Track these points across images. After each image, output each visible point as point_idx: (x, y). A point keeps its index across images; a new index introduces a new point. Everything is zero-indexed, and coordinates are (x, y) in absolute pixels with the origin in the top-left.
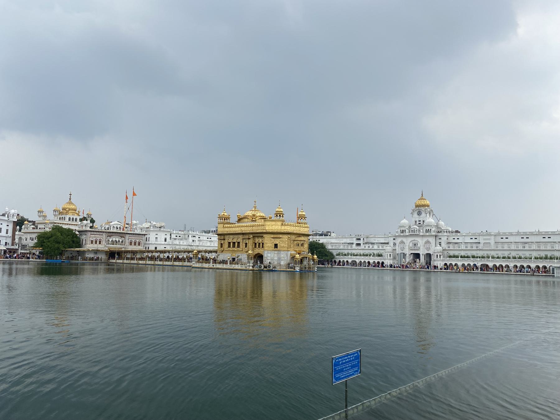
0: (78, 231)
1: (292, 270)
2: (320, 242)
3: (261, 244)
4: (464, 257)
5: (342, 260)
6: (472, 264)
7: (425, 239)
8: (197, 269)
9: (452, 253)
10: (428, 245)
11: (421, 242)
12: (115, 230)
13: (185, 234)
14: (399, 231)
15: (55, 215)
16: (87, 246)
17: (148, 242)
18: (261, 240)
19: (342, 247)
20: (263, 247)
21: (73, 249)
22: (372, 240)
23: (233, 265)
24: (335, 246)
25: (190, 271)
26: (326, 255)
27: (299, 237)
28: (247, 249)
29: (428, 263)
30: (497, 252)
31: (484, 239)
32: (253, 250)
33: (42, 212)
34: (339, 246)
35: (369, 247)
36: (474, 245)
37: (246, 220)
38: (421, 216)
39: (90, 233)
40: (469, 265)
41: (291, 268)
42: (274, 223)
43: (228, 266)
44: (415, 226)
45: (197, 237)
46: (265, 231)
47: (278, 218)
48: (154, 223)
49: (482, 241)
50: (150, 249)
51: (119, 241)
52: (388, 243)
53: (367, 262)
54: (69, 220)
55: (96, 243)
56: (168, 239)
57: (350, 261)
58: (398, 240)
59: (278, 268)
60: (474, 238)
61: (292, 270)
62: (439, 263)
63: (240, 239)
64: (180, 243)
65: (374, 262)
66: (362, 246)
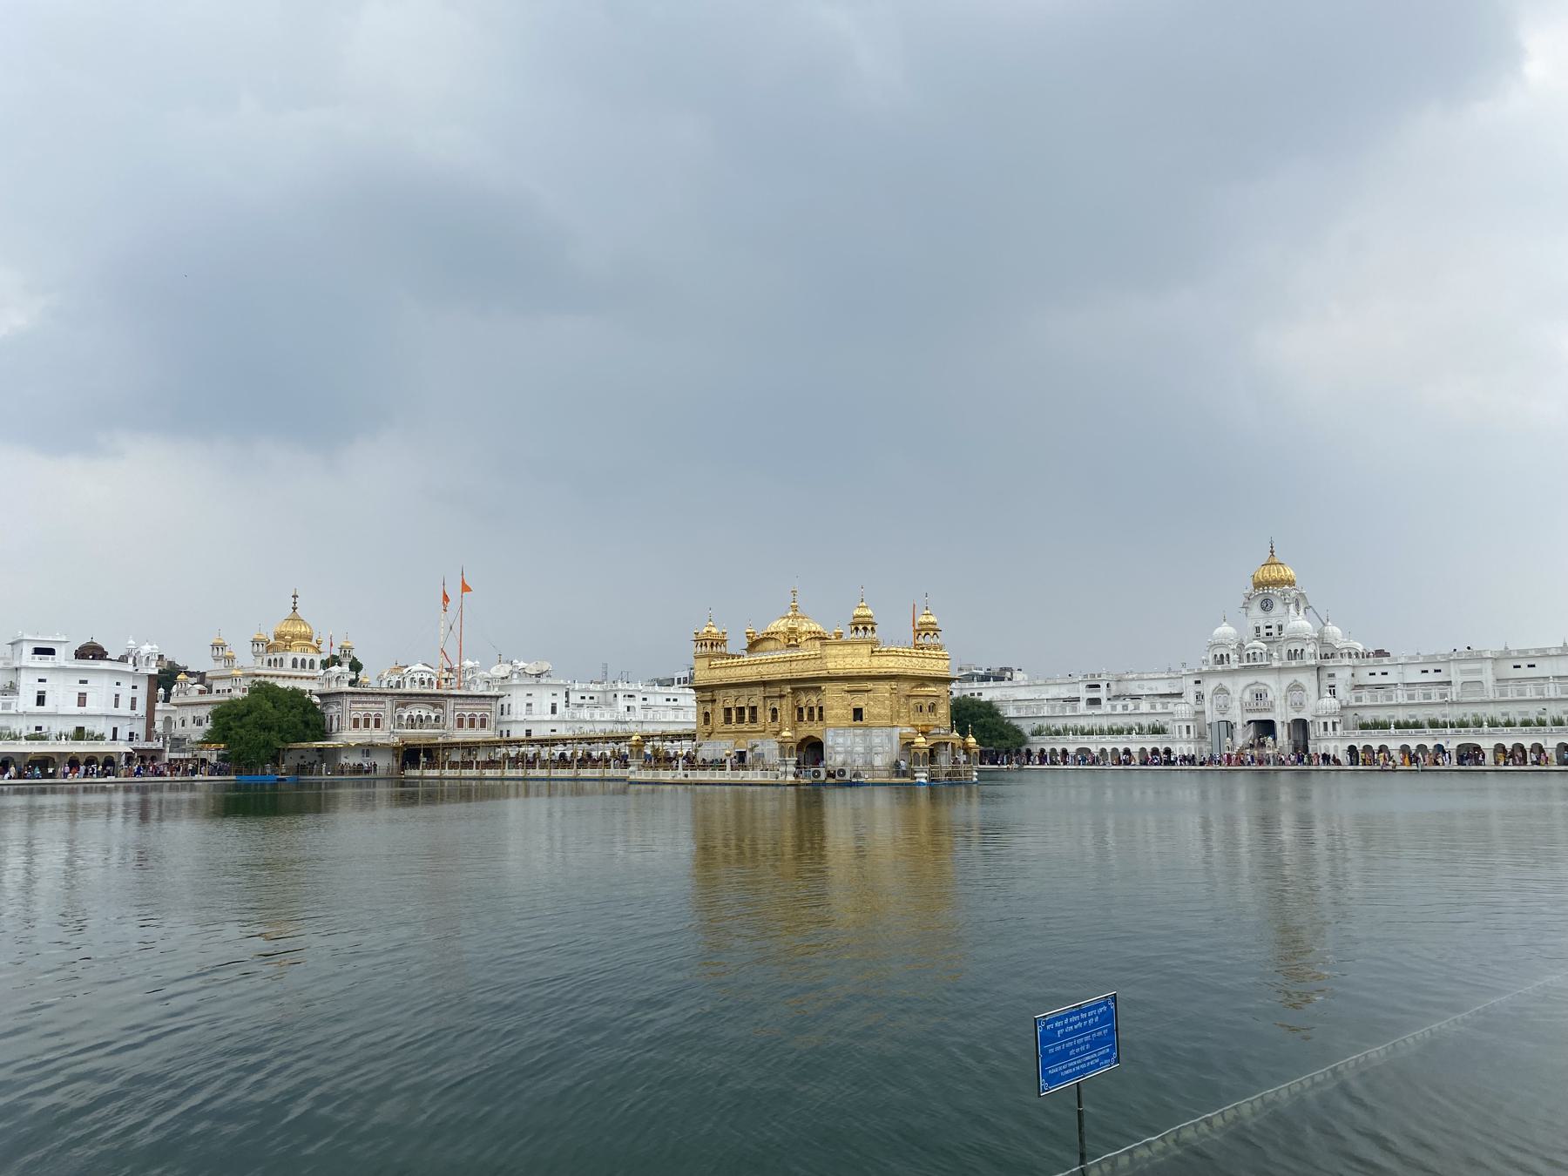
0: (320, 696)
1: (908, 780)
2: (984, 698)
3: (816, 711)
4: (1407, 726)
5: (1048, 749)
6: (1430, 745)
7: (1287, 679)
8: (643, 787)
9: (1368, 716)
10: (1296, 696)
11: (1275, 687)
12: (417, 689)
13: (605, 692)
14: (1211, 657)
15: (256, 655)
16: (345, 733)
17: (506, 718)
18: (814, 699)
19: (1046, 711)
20: (821, 718)
21: (304, 744)
22: (1134, 688)
23: (742, 773)
25: (625, 792)
26: (1002, 736)
27: (923, 685)
28: (776, 724)
29: (1301, 749)
30: (1503, 708)
31: (1463, 672)
32: (794, 729)
33: (223, 646)
34: (1039, 708)
35: (1125, 707)
36: (1435, 694)
37: (771, 644)
38: (1273, 613)
39: (349, 699)
40: (1422, 748)
41: (904, 774)
42: (848, 649)
43: (727, 775)
44: (1256, 643)
45: (639, 697)
46: (824, 673)
47: (861, 634)
48: (522, 665)
49: (1457, 678)
50: (513, 736)
51: (428, 717)
52: (1179, 695)
53: (1059, 750)
54: (294, 665)
55: (367, 725)
56: (561, 708)
57: (1072, 749)
58: (1209, 686)
59: (866, 777)
60: (1431, 668)
61: (908, 780)
63: (756, 698)
64: (592, 715)
65: (1143, 750)
66: (1106, 707)
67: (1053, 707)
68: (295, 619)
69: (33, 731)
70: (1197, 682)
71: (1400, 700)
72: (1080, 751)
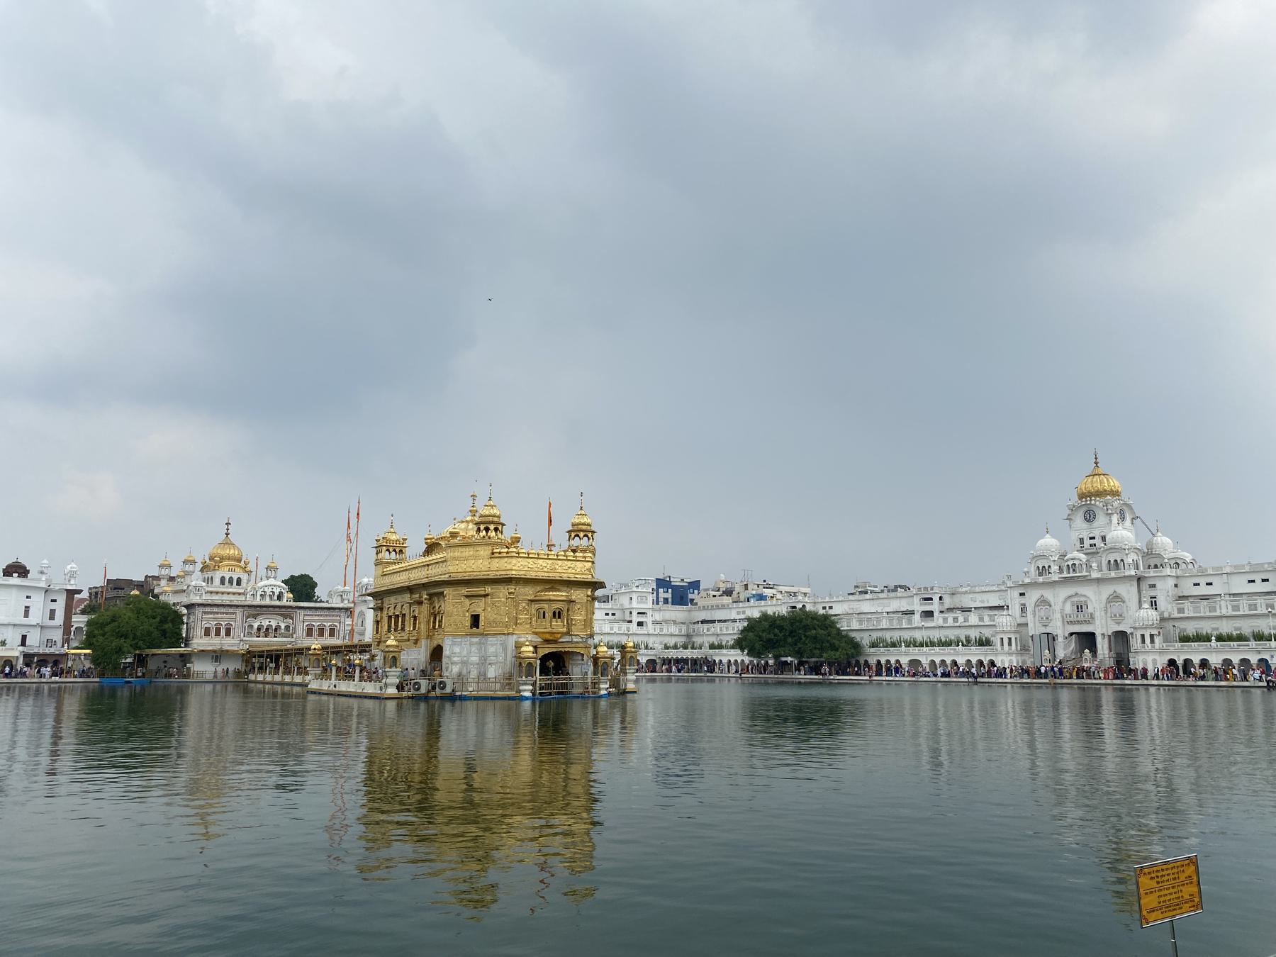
4: (1230, 638)
5: (883, 662)
7: (1107, 591)
9: (1191, 628)
10: (1116, 608)
11: (1095, 598)
12: (267, 602)
14: (1033, 569)
16: (195, 641)
19: (885, 624)
22: (967, 601)
24: (869, 620)
26: (834, 648)
32: (429, 637)
34: (879, 621)
35: (956, 620)
38: (1096, 524)
39: (201, 609)
40: (1245, 661)
42: (468, 552)
44: (1076, 554)
54: (222, 581)
55: (218, 632)
58: (1033, 596)
59: (471, 690)
62: (1150, 658)
66: (938, 620)
67: (891, 620)
68: (227, 543)
71: (1224, 612)
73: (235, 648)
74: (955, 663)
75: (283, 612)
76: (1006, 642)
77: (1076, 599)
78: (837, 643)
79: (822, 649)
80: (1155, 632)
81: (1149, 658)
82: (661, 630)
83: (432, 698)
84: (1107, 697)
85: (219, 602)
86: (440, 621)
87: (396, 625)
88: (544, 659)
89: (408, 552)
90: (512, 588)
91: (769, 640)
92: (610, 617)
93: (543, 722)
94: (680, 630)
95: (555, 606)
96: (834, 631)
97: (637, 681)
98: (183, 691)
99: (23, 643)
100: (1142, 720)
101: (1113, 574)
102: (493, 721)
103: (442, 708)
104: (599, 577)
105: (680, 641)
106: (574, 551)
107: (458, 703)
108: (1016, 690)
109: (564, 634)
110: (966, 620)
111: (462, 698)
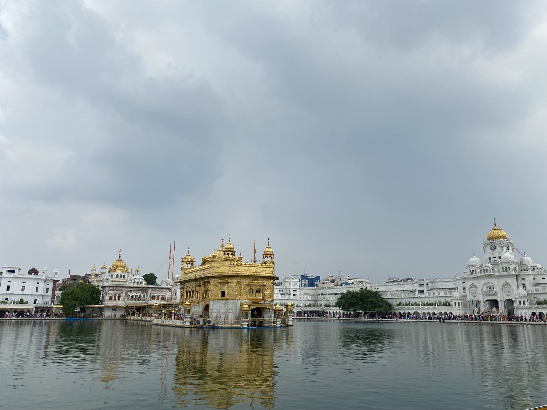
5: (402, 313)
7: (502, 281)
10: (507, 289)
11: (497, 284)
12: (136, 285)
19: (402, 296)
22: (439, 286)
24: (395, 294)
26: (380, 306)
32: (204, 301)
34: (400, 295)
35: (434, 294)
38: (496, 251)
42: (220, 264)
44: (487, 265)
54: (117, 276)
55: (115, 298)
57: (412, 312)
58: (468, 284)
59: (221, 324)
66: (426, 294)
67: (405, 294)
68: (120, 260)
69: (4, 300)
70: (464, 283)
72: (415, 312)
73: (122, 305)
74: (434, 313)
75: (142, 289)
76: (457, 304)
77: (488, 285)
78: (381, 304)
79: (375, 307)
80: (525, 300)
81: (523, 311)
82: (303, 298)
83: (205, 328)
84: (505, 330)
85: (116, 285)
86: (208, 294)
87: (190, 296)
88: (253, 311)
89: (195, 264)
90: (239, 280)
91: (351, 303)
92: (281, 292)
93: (252, 340)
94: (312, 298)
95: (257, 287)
96: (380, 299)
97: (293, 321)
98: (100, 324)
99: (35, 303)
100: (521, 339)
101: (505, 274)
102: (231, 338)
103: (209, 332)
104: (276, 275)
105: (312, 303)
106: (265, 263)
107: (216, 329)
108: (463, 325)
109: (261, 300)
110: (439, 294)
111: (217, 328)
